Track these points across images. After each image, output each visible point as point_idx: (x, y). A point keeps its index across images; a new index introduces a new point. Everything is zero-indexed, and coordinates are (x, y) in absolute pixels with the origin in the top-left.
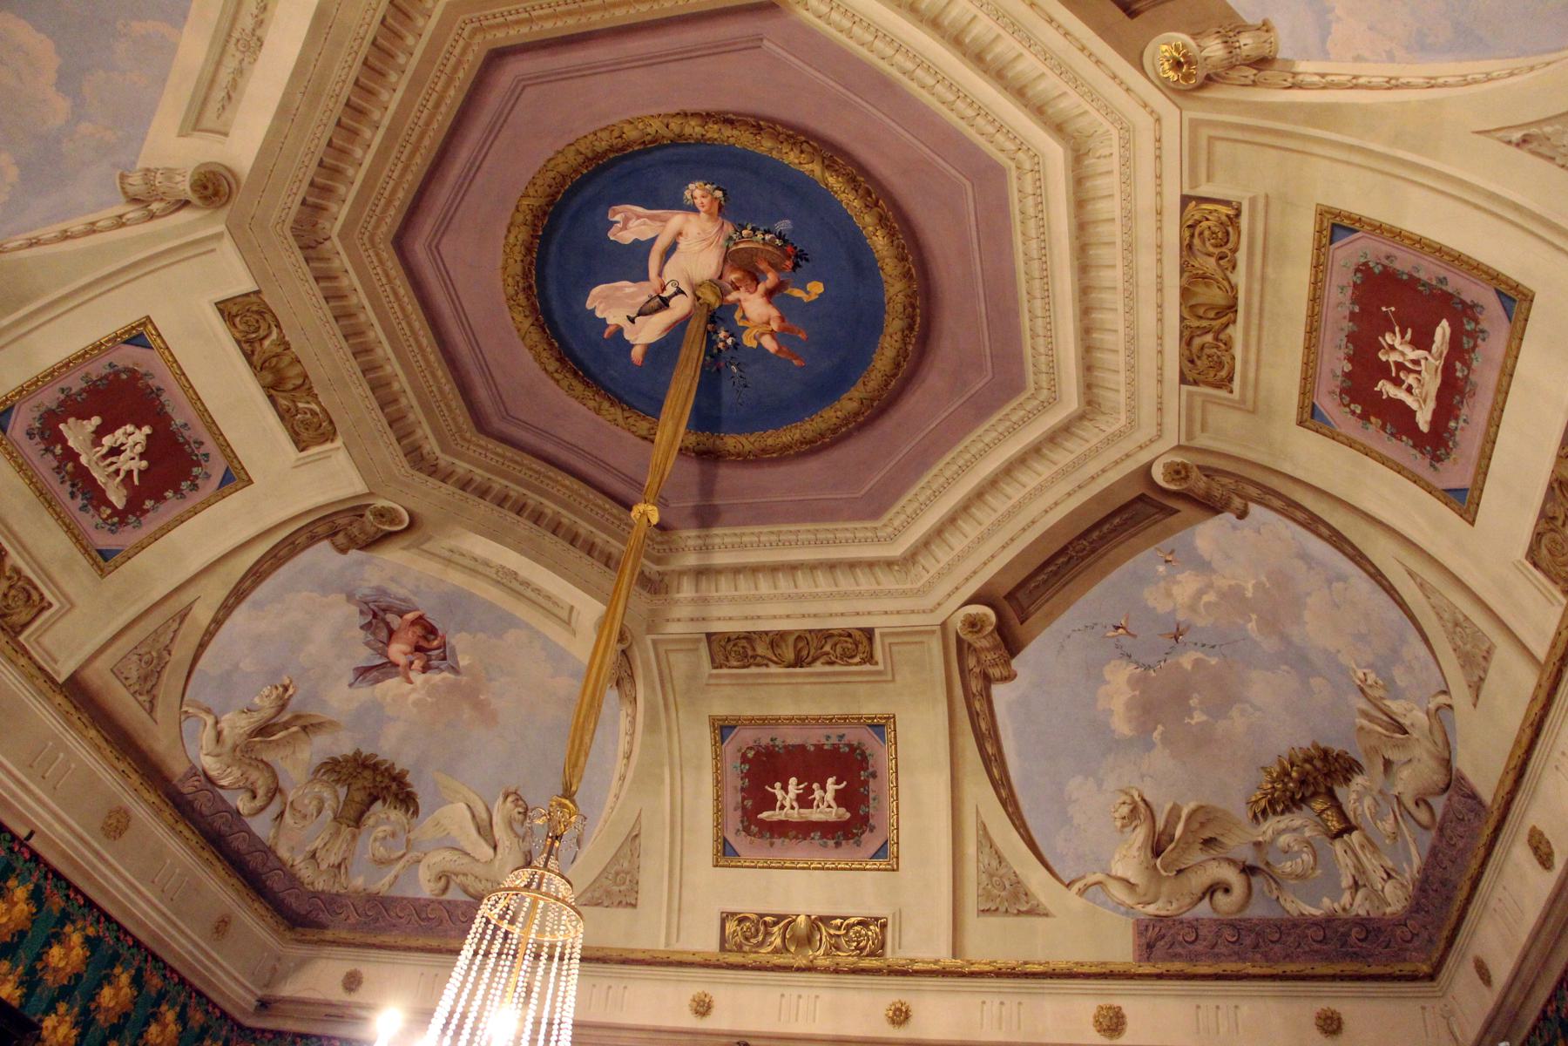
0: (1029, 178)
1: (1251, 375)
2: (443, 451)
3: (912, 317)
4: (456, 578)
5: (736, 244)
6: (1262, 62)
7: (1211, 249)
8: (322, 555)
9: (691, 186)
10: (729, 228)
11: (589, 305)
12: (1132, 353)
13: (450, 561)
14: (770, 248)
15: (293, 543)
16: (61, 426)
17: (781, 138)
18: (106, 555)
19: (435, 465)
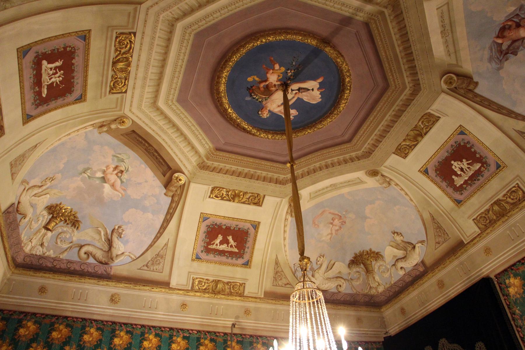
0: (170, 98)
1: (108, 42)
2: (406, 88)
3: (224, 64)
4: (463, 43)
5: (265, 98)
6: (102, 126)
7: (119, 80)
8: (482, 90)
9: (265, 117)
10: (264, 103)
11: (321, 100)
12: (152, 44)
13: (455, 52)
14: (257, 93)
15: (481, 102)
16: (458, 186)
17: (233, 121)
18: (498, 166)
19: (414, 86)
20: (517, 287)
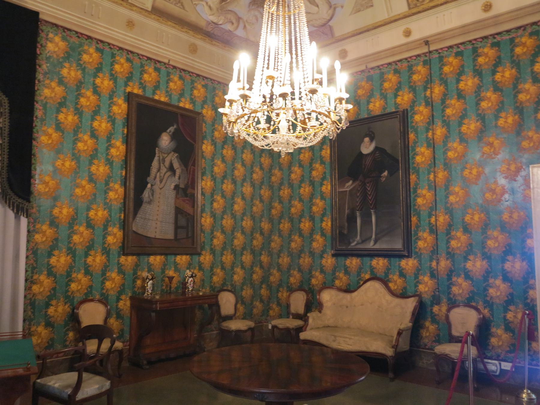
20: (59, 48)
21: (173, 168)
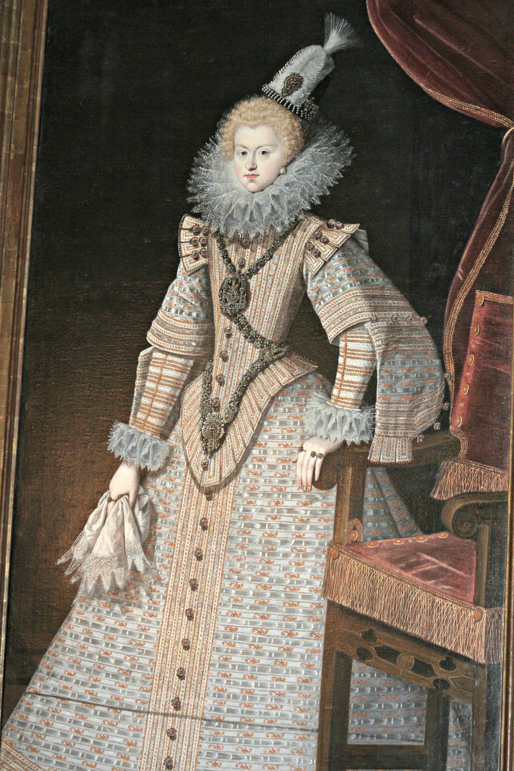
21: (322, 332)
